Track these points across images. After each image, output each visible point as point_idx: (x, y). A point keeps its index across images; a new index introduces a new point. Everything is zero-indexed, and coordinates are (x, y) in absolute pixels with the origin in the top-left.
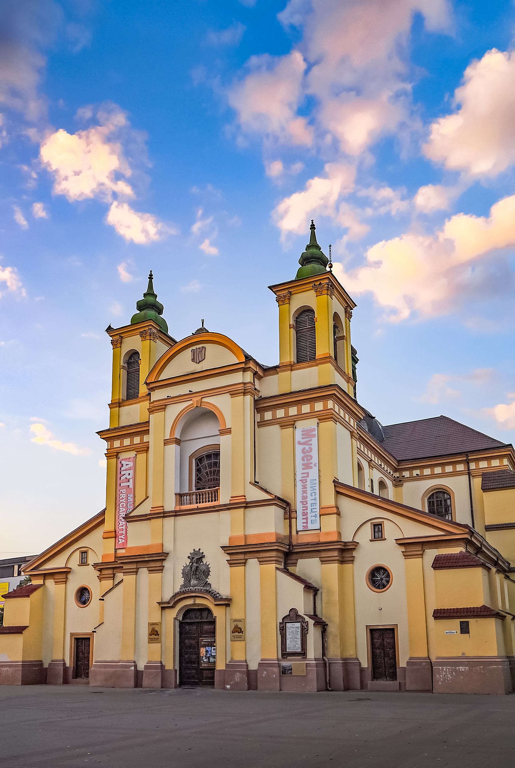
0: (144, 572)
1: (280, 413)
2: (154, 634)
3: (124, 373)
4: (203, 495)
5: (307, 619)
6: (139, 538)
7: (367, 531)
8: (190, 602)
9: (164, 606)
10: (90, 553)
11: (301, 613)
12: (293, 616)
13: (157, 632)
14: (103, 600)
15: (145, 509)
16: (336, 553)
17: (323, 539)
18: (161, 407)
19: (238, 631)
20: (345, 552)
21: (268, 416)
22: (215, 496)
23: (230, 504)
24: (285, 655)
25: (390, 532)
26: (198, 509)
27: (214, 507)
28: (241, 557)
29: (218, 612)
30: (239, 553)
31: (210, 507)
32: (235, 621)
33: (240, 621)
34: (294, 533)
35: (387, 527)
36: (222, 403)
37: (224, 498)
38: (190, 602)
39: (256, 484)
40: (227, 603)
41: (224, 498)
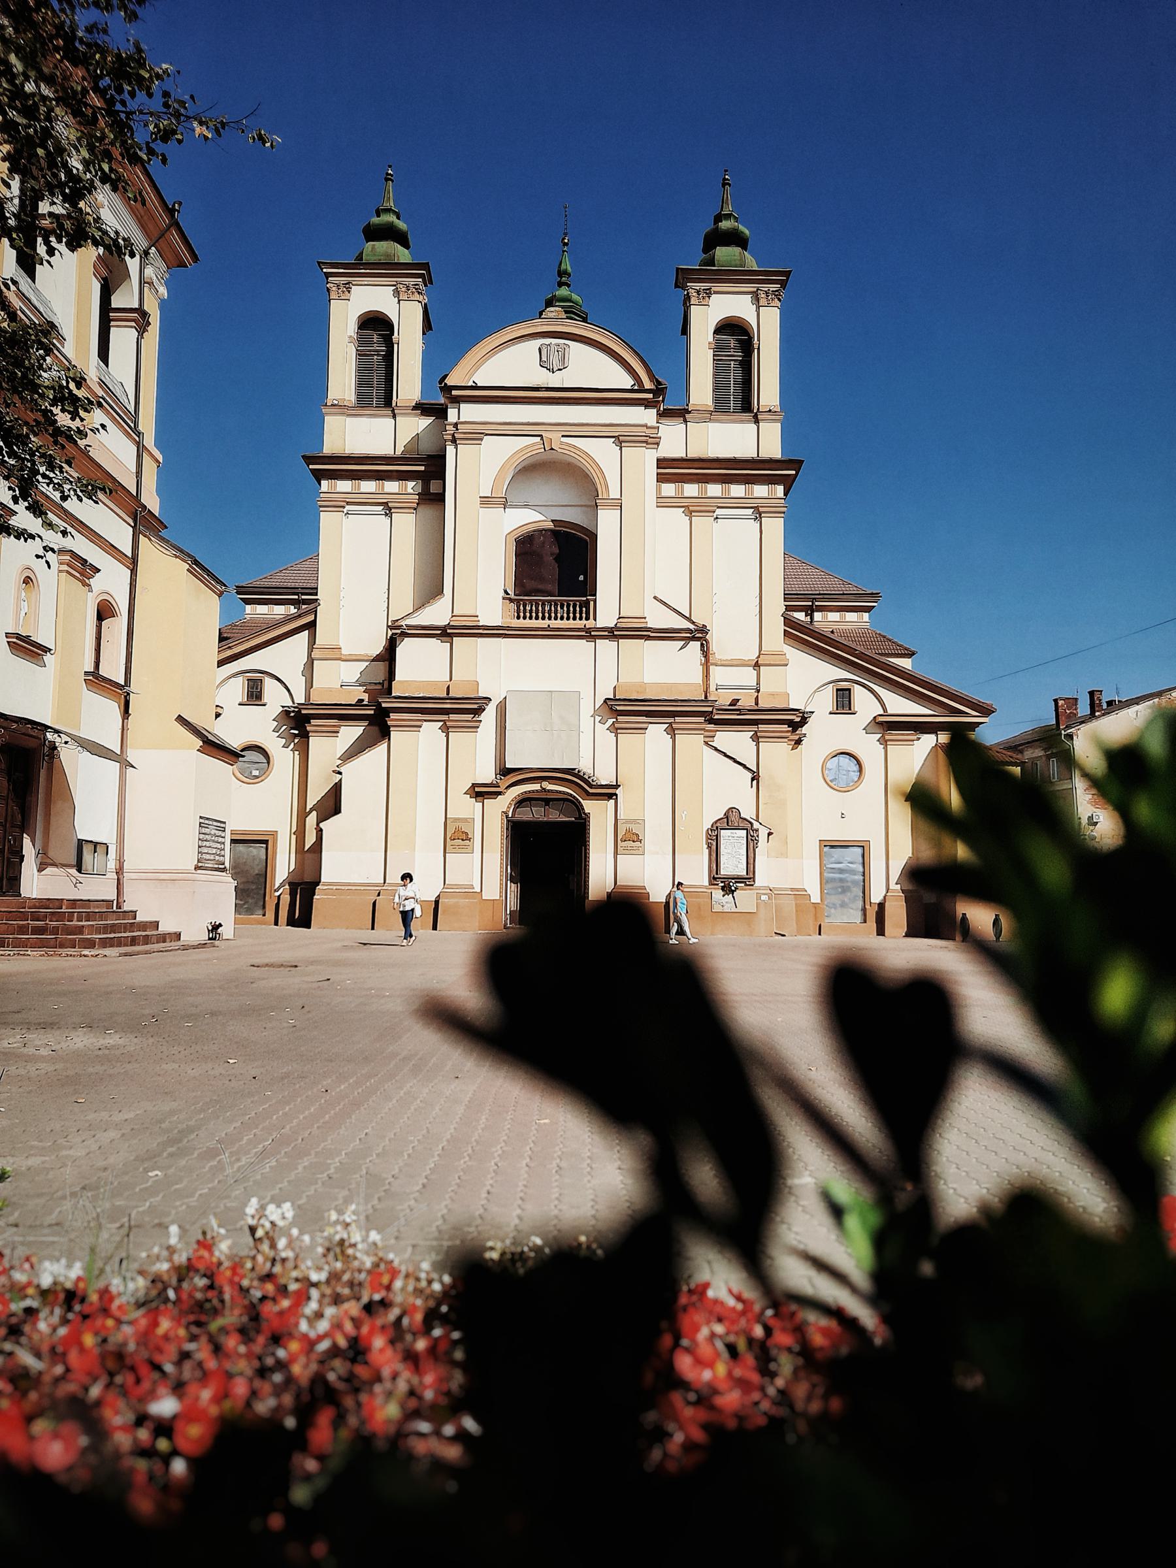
0: (431, 730)
1: (691, 490)
2: (456, 837)
3: (352, 351)
4: (543, 605)
5: (756, 825)
6: (420, 667)
7: (828, 698)
8: (536, 787)
9: (480, 793)
10: (269, 683)
11: (748, 813)
12: (731, 819)
13: (467, 834)
14: (340, 773)
15: (437, 614)
16: (785, 727)
17: (763, 704)
19: (628, 839)
21: (669, 489)
22: (587, 609)
23: (616, 628)
25: (866, 704)
26: (549, 629)
29: (589, 806)
30: (625, 711)
31: (579, 630)
32: (628, 821)
33: (635, 821)
34: (712, 688)
35: (860, 696)
38: (536, 787)
39: (655, 598)
40: (609, 793)
41: (605, 616)
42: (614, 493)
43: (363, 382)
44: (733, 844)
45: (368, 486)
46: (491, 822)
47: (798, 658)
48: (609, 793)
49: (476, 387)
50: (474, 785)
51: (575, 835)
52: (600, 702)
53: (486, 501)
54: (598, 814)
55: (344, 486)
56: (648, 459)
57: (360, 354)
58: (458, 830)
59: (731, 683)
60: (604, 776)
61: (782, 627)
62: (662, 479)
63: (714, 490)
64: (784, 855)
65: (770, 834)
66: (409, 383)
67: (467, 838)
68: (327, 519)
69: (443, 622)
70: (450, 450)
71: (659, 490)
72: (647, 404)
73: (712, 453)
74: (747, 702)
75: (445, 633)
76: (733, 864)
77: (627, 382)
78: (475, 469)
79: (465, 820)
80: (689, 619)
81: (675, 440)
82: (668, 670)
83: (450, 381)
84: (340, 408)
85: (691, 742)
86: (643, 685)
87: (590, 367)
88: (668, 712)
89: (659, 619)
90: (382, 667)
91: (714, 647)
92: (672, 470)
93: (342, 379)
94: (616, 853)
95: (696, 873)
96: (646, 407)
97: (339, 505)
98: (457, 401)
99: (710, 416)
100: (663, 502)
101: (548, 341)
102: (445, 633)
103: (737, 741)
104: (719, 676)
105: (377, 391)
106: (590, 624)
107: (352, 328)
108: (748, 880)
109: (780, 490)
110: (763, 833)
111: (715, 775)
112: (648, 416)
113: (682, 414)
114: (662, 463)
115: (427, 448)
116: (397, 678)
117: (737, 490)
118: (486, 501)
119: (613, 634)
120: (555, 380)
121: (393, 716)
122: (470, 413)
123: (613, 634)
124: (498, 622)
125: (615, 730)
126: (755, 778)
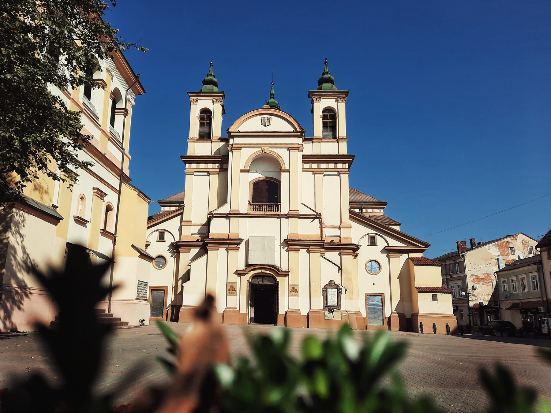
0: (222, 250)
1: (315, 166)
2: (231, 289)
6: (219, 228)
8: (259, 271)
9: (239, 273)
11: (338, 282)
12: (331, 285)
15: (225, 209)
16: (351, 251)
17: (342, 242)
18: (239, 148)
19: (293, 291)
20: (354, 249)
21: (307, 166)
23: (288, 214)
24: (326, 306)
26: (264, 214)
27: (278, 215)
28: (298, 247)
29: (279, 279)
30: (292, 244)
32: (293, 285)
33: (296, 285)
34: (324, 236)
36: (282, 154)
37: (284, 210)
38: (259, 271)
41: (284, 210)
42: (287, 167)
43: (201, 131)
44: (332, 293)
45: (202, 166)
46: (243, 284)
47: (354, 224)
48: (286, 274)
49: (239, 132)
50: (237, 271)
51: (274, 289)
52: (282, 241)
53: (242, 171)
54: (282, 282)
55: (194, 166)
56: (298, 156)
57: (200, 122)
58: (231, 287)
59: (330, 234)
60: (284, 268)
61: (349, 214)
62: (304, 162)
63: (323, 166)
64: (351, 298)
65: (346, 290)
66: (217, 131)
67: (234, 290)
68: (188, 177)
69: (227, 212)
70: (230, 153)
71: (303, 166)
72: (298, 137)
73: (322, 153)
74: (336, 241)
75: (227, 216)
76: (332, 301)
77: (292, 129)
78: (239, 160)
79: (234, 283)
80: (315, 211)
81: (309, 149)
82: (307, 229)
83: (230, 130)
84: (193, 140)
85: (316, 255)
86: (298, 235)
87: (279, 124)
88: (308, 245)
89: (304, 211)
90: (206, 228)
91: (324, 221)
92: (307, 159)
93: (194, 130)
94: (289, 296)
95: (318, 304)
96: (298, 138)
97: (192, 172)
98: (233, 137)
99: (321, 140)
100: (304, 170)
101: (264, 116)
102: (227, 216)
103: (333, 256)
104: (326, 231)
105: (206, 134)
106: (279, 213)
107: (198, 113)
108: (338, 307)
109: (347, 166)
110: (343, 290)
111: (325, 268)
112: (299, 141)
113: (311, 140)
114: (304, 156)
115: (222, 153)
116: (211, 232)
117: (331, 166)
118: (242, 171)
119: (287, 216)
120: (266, 129)
121: (209, 245)
122: (237, 140)
123: (287, 216)
124: (245, 212)
125: (288, 250)
126: (340, 269)
